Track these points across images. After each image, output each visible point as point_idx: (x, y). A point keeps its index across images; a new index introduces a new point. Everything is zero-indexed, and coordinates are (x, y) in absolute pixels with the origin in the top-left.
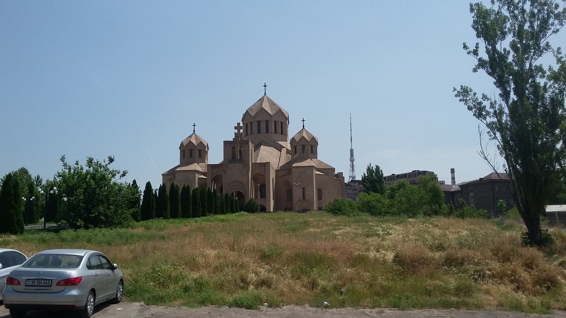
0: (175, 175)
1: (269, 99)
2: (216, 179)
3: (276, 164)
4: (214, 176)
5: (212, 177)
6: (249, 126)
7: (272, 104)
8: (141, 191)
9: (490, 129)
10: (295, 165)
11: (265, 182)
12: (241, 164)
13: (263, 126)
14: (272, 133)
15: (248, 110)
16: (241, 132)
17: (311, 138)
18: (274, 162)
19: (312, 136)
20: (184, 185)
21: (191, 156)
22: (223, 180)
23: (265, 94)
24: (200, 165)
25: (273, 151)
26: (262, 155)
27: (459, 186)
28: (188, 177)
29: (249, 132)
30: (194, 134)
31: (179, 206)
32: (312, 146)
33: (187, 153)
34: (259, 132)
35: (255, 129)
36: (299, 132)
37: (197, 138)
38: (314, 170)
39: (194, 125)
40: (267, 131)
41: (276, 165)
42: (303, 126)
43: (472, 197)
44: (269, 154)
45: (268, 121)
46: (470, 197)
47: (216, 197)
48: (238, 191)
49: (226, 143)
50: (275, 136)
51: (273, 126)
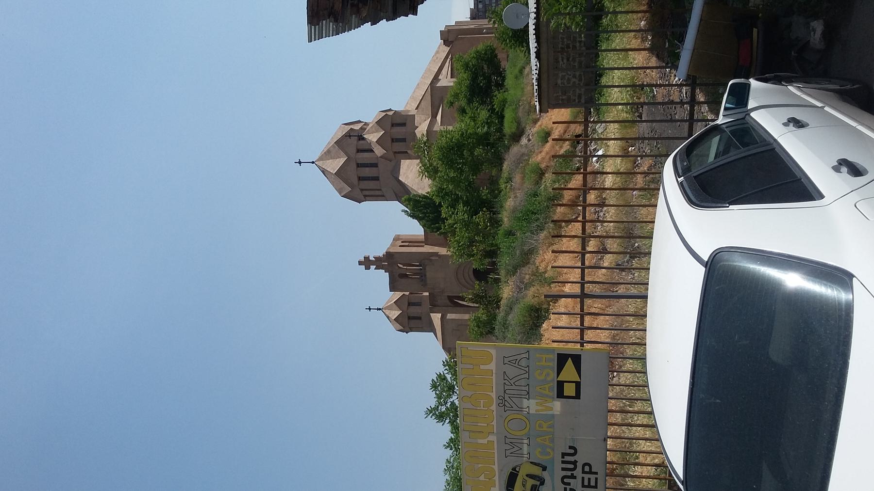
6: (367, 193)
7: (328, 154)
13: (367, 172)
19: (376, 125)
23: (313, 162)
29: (378, 193)
30: (384, 310)
32: (393, 125)
33: (413, 323)
34: (376, 179)
35: (371, 184)
37: (389, 308)
39: (370, 309)
44: (412, 167)
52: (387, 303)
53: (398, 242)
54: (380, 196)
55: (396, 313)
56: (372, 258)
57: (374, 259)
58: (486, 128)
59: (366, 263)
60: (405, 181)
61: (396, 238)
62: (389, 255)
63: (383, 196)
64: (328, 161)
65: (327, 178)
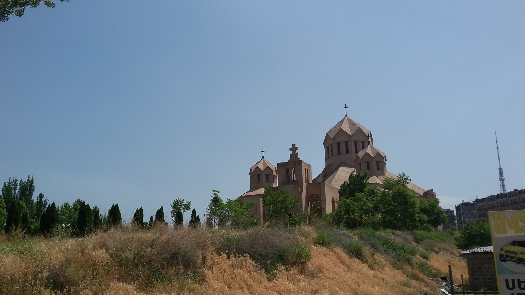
6: (330, 148)
7: (352, 124)
13: (343, 147)
14: (352, 153)
15: (328, 133)
17: (376, 153)
20: (113, 204)
23: (346, 115)
26: (339, 176)
32: (377, 162)
34: (339, 153)
35: (335, 151)
37: (264, 163)
40: (347, 152)
45: (348, 142)
51: (353, 146)
52: (267, 162)
53: (308, 167)
54: (328, 156)
55: (261, 167)
56: (297, 152)
57: (296, 153)
58: (418, 219)
59: (294, 148)
60: (339, 171)
61: (309, 166)
62: (300, 162)
63: (328, 157)
64: (348, 124)
65: (337, 124)
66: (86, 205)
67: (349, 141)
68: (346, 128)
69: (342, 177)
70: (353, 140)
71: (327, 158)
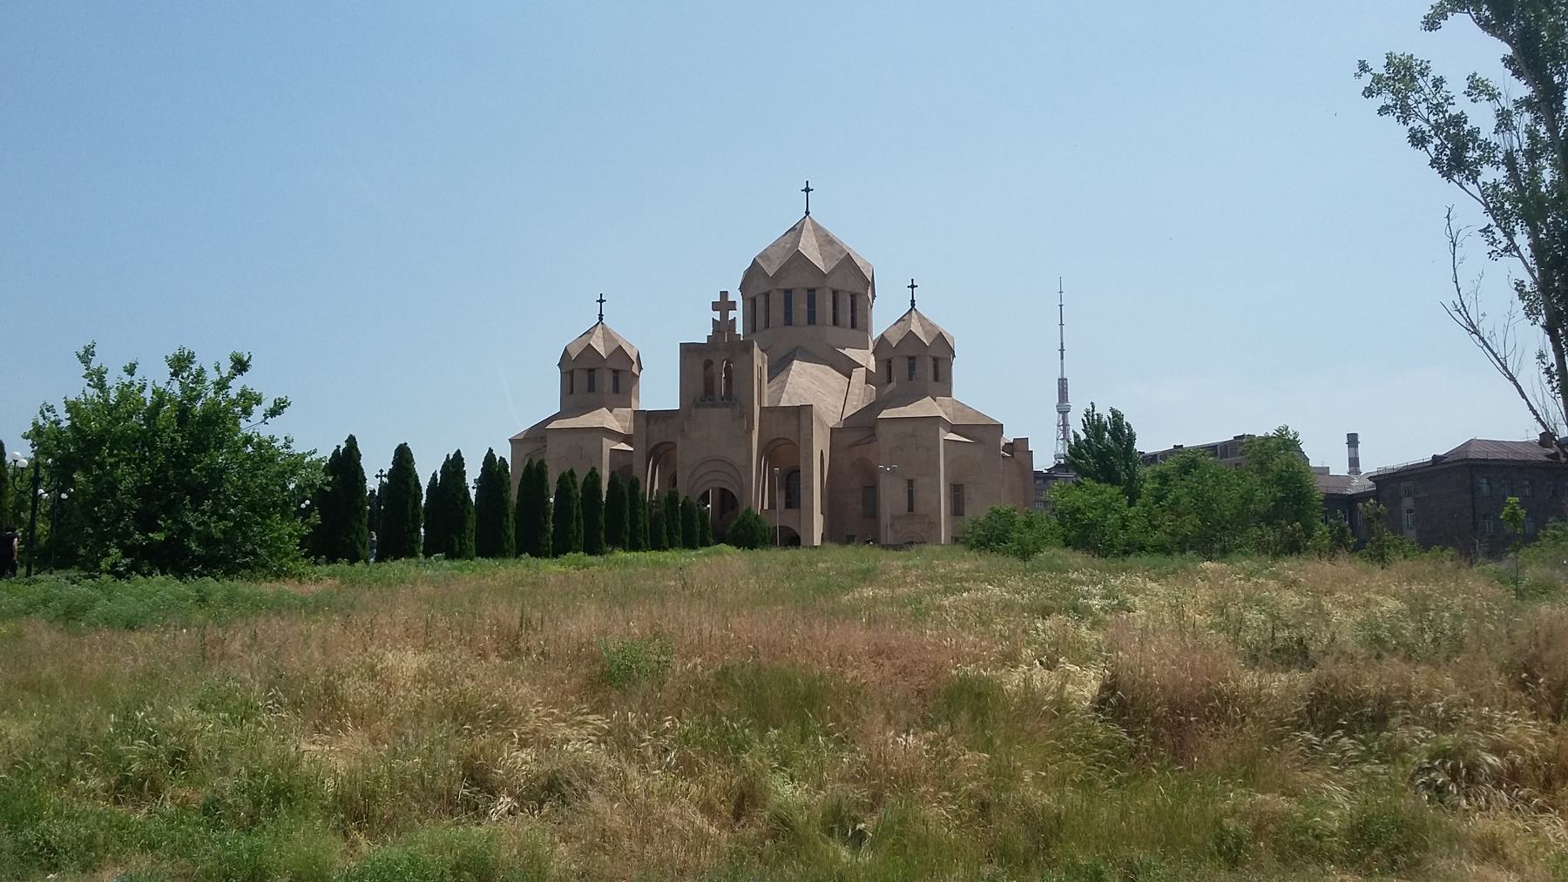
0: (546, 441)
1: (816, 227)
2: (661, 454)
3: (834, 412)
4: (652, 446)
5: (647, 448)
6: (760, 303)
7: (827, 241)
8: (379, 474)
9: (1494, 219)
10: (886, 414)
11: (799, 462)
12: (728, 410)
13: (801, 306)
14: (825, 325)
15: (758, 260)
16: (730, 319)
18: (829, 408)
21: (591, 388)
22: (678, 454)
23: (807, 213)
24: (617, 415)
25: (827, 374)
26: (796, 387)
27: (1370, 478)
28: (582, 448)
29: (760, 323)
30: (600, 325)
31: (508, 521)
32: (935, 359)
33: (581, 380)
34: (788, 321)
35: (778, 312)
36: (898, 321)
37: (608, 336)
38: (940, 428)
39: (601, 301)
41: (835, 415)
42: (913, 302)
43: (1409, 511)
46: (1405, 515)
47: (638, 499)
48: (724, 489)
49: (687, 350)
50: (832, 333)
63: (754, 330)
64: (814, 239)
65: (784, 236)
66: (498, 459)
67: (821, 288)
68: (811, 249)
69: (803, 389)
70: (829, 288)
71: (750, 331)
